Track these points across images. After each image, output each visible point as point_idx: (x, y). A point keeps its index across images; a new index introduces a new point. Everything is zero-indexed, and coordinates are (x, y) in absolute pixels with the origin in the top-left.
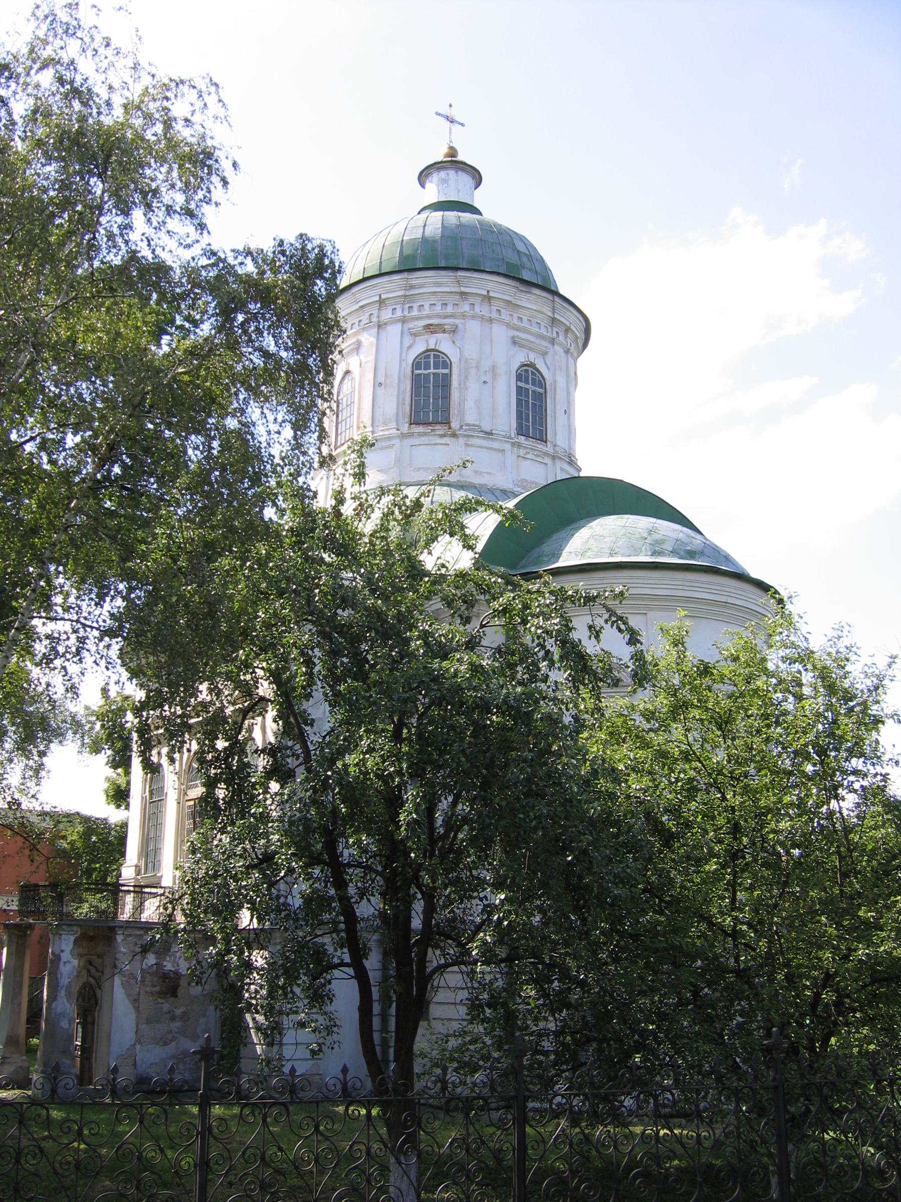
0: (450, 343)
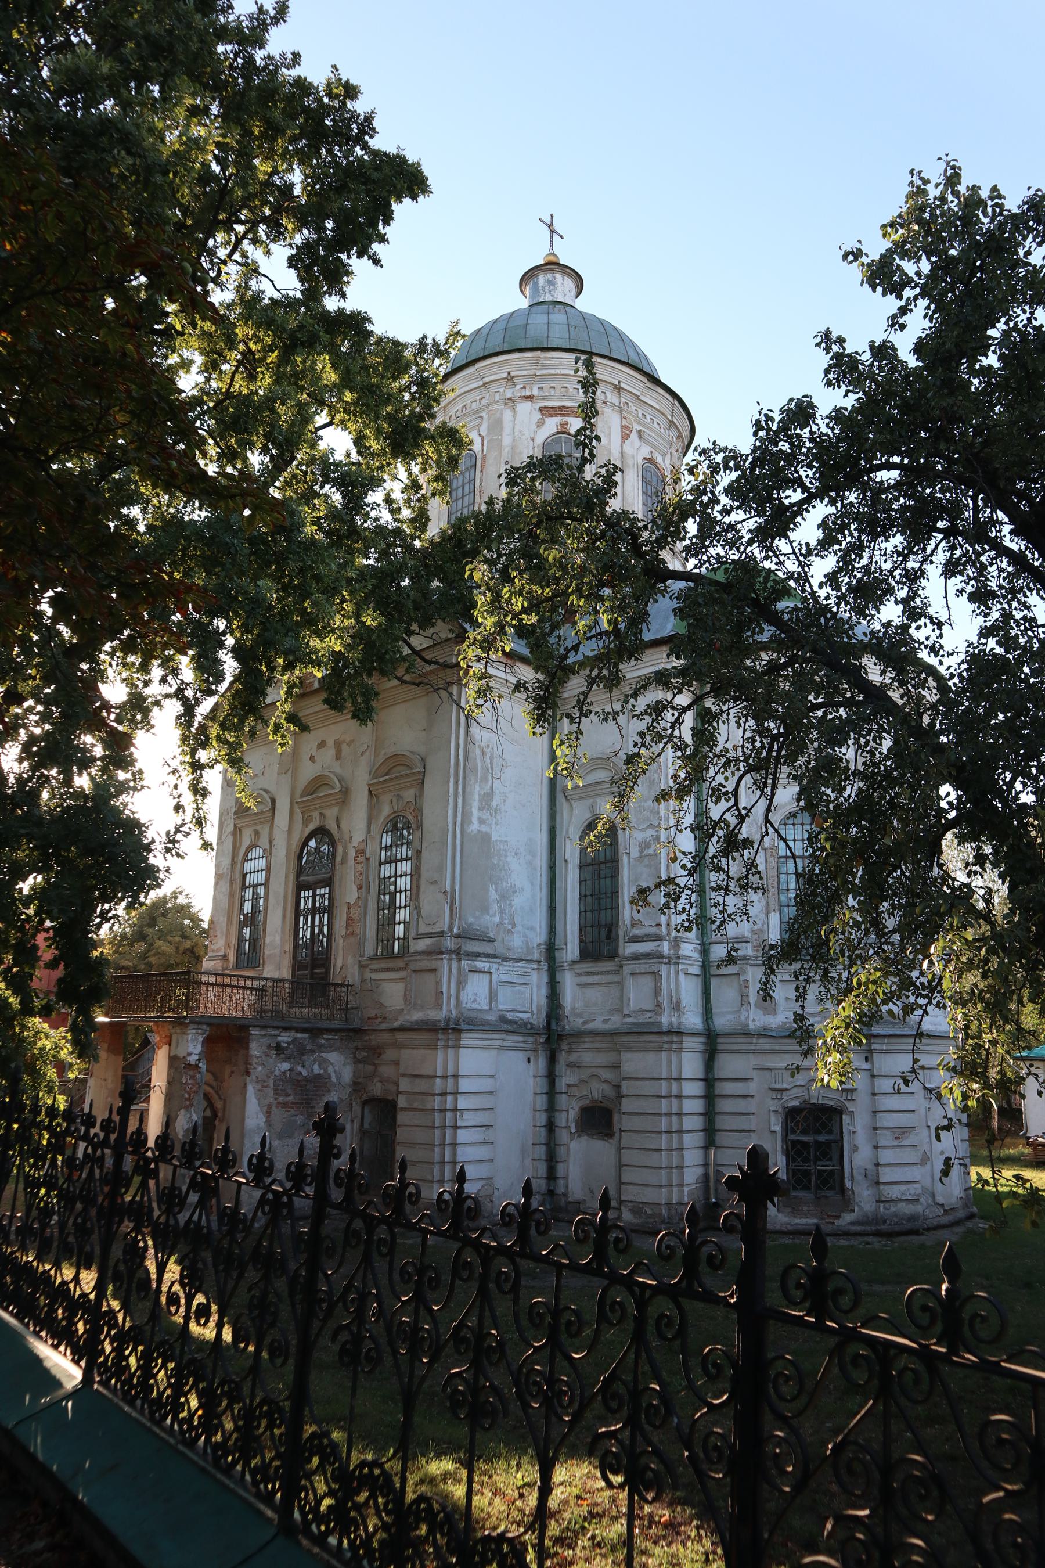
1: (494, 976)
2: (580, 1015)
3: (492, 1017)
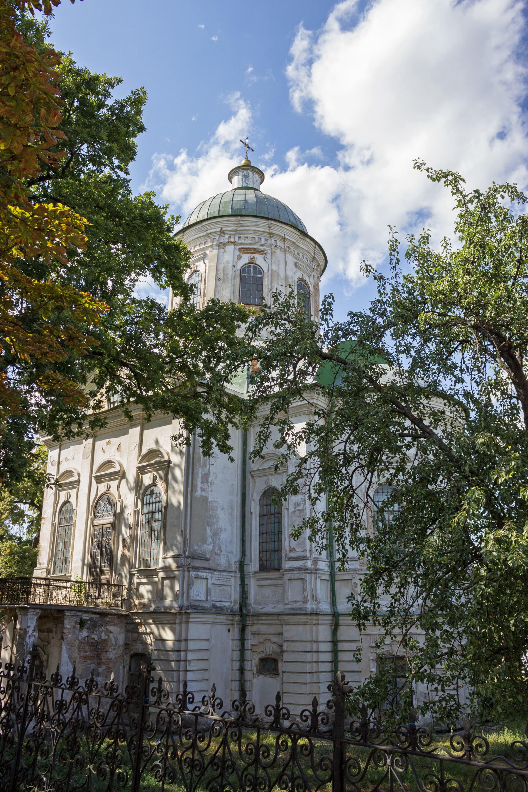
1: (210, 581)
2: (259, 604)
3: (208, 605)
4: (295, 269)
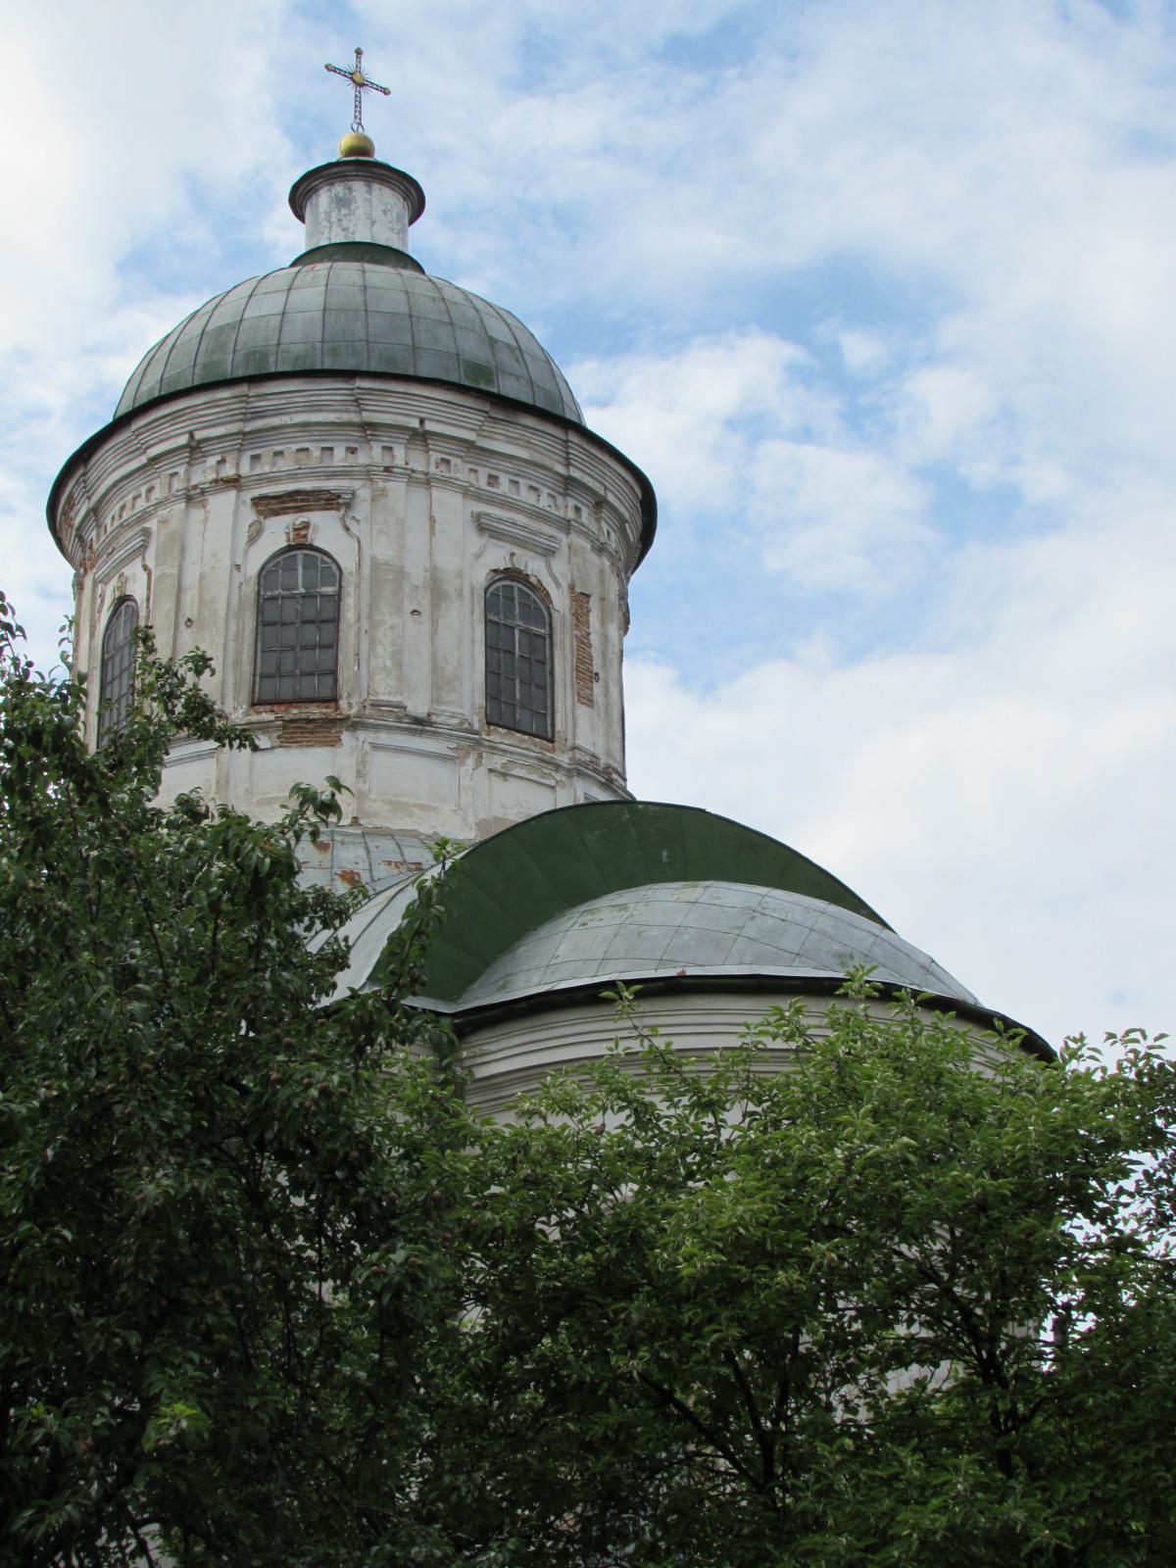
0: (341, 531)
4: (476, 541)
